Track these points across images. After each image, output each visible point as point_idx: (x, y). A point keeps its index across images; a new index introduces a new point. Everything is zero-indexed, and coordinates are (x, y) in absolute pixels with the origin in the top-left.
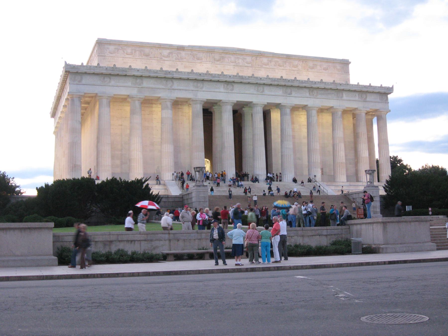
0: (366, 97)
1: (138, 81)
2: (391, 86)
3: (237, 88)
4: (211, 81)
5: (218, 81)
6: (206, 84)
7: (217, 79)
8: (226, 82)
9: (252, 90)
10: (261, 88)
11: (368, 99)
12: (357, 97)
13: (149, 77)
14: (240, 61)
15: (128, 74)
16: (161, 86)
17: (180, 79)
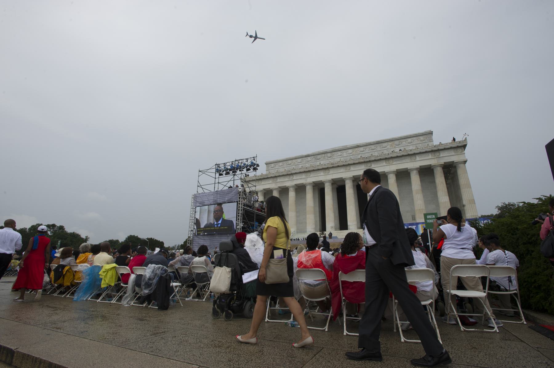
0: (440, 155)
1: (275, 179)
2: (464, 139)
3: (331, 171)
4: (314, 170)
5: (318, 170)
6: (312, 172)
7: (317, 168)
8: (323, 169)
9: (342, 170)
10: (348, 168)
11: (441, 155)
12: (430, 156)
13: (279, 176)
14: (345, 153)
15: (269, 176)
16: (287, 179)
17: (296, 173)
